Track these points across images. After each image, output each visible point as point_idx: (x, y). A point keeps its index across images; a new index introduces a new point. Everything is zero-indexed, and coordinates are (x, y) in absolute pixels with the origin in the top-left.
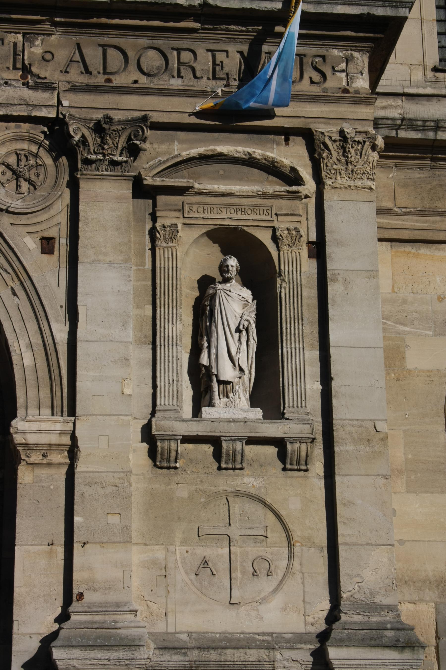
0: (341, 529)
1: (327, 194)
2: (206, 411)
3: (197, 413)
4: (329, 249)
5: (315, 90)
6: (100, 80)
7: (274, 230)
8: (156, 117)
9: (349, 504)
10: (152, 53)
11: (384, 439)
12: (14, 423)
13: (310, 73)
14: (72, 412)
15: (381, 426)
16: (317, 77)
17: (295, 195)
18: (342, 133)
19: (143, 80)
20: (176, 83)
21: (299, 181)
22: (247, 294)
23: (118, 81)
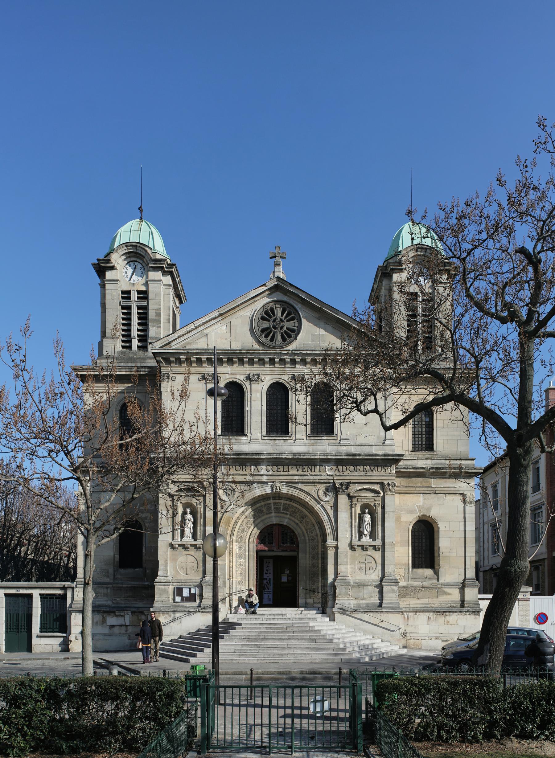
0: (386, 562)
1: (386, 496)
2: (362, 540)
3: (359, 540)
4: (386, 507)
5: (384, 474)
6: (341, 473)
7: (375, 504)
8: (352, 481)
9: (387, 557)
10: (352, 467)
11: (394, 545)
12: (327, 543)
13: (383, 470)
14: (337, 540)
15: (394, 542)
16: (384, 471)
17: (379, 496)
18: (389, 483)
19: (350, 473)
20: (356, 473)
21: (380, 494)
22: (369, 516)
23: (346, 473)
